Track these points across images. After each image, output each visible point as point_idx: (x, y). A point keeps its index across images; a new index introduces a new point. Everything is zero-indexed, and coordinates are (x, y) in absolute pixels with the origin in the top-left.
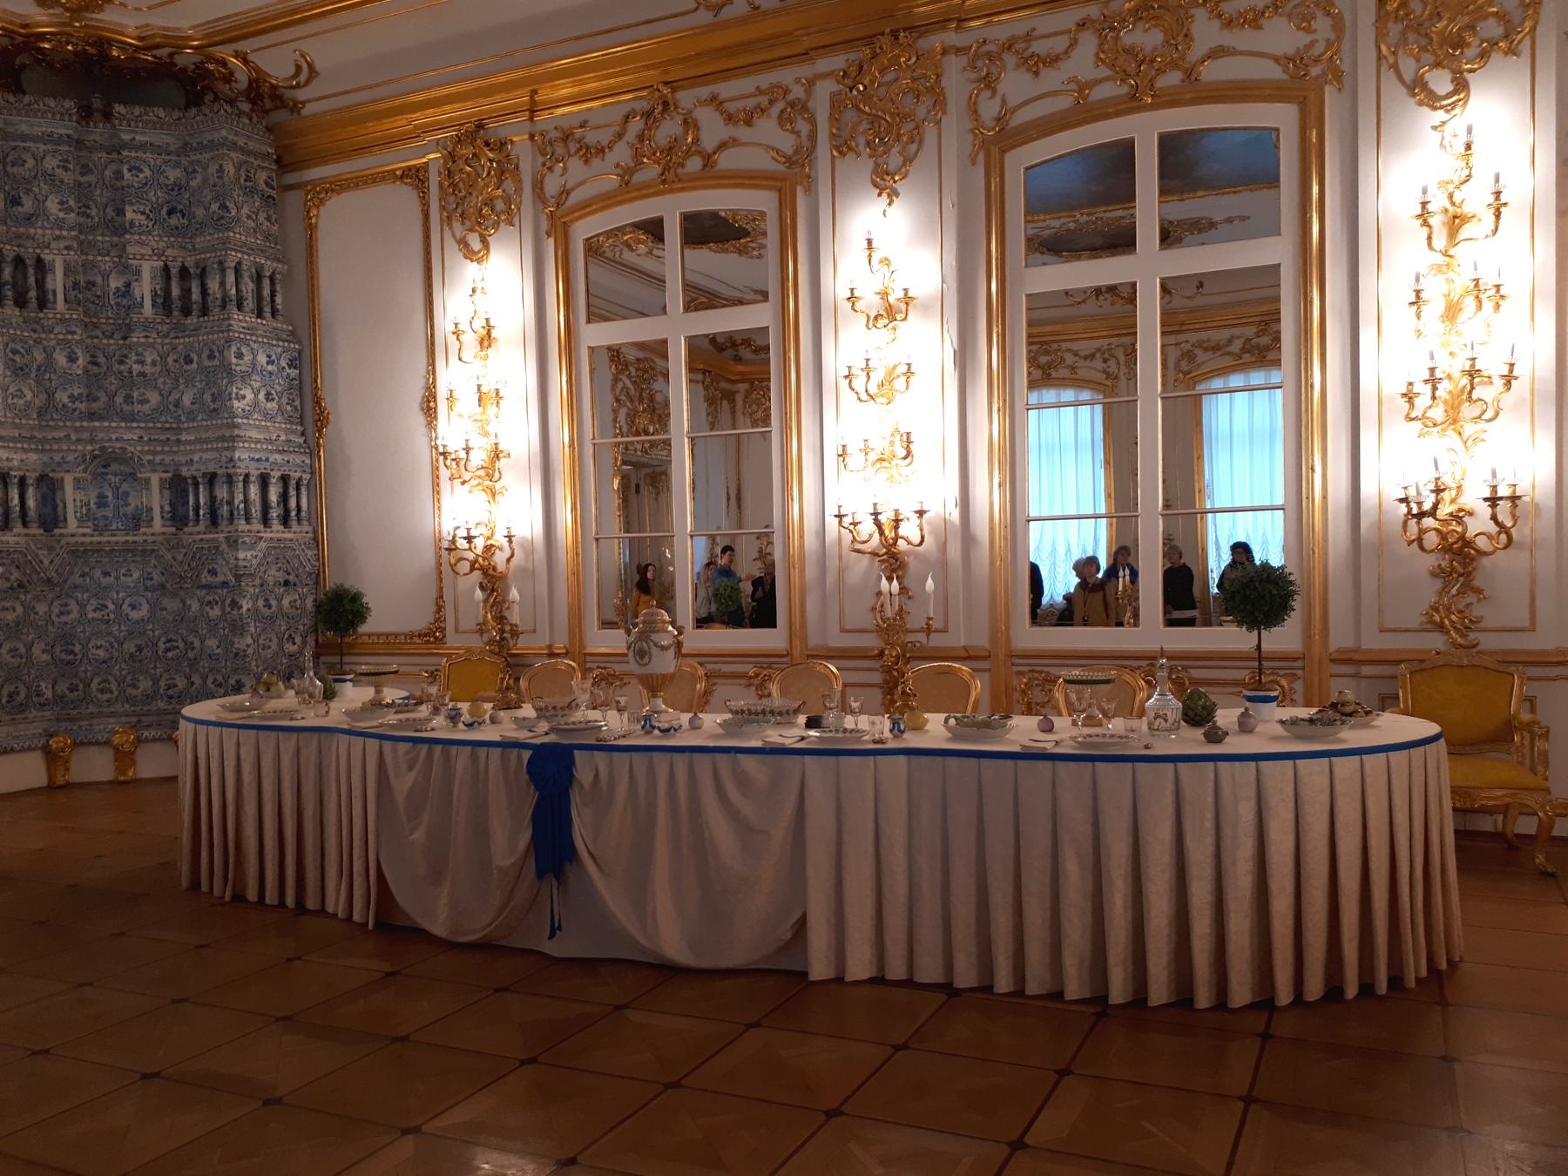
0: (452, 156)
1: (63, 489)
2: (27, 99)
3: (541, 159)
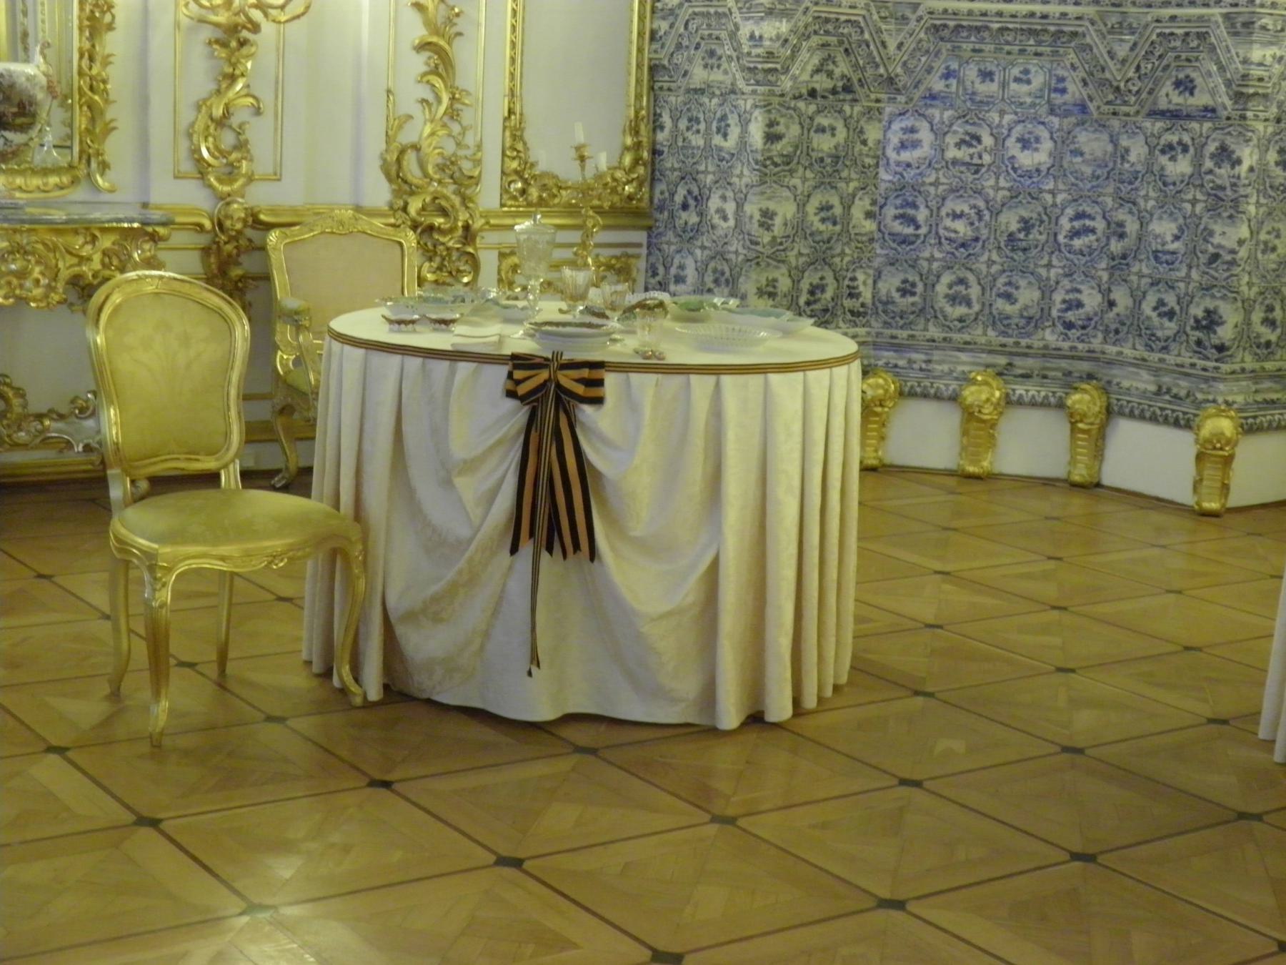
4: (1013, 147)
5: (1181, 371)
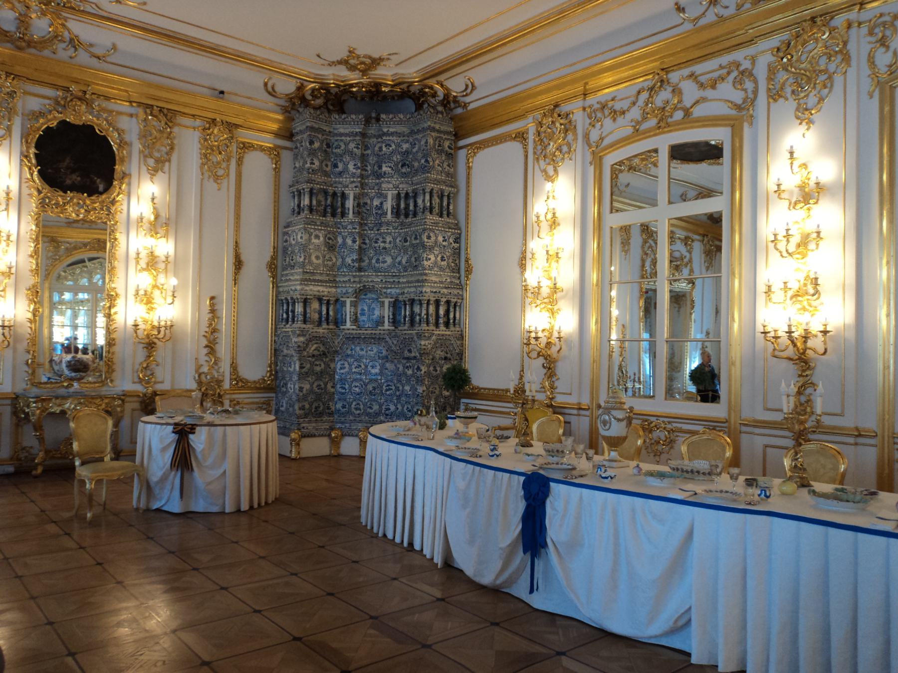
0: (541, 124)
3: (588, 121)
4: (369, 368)
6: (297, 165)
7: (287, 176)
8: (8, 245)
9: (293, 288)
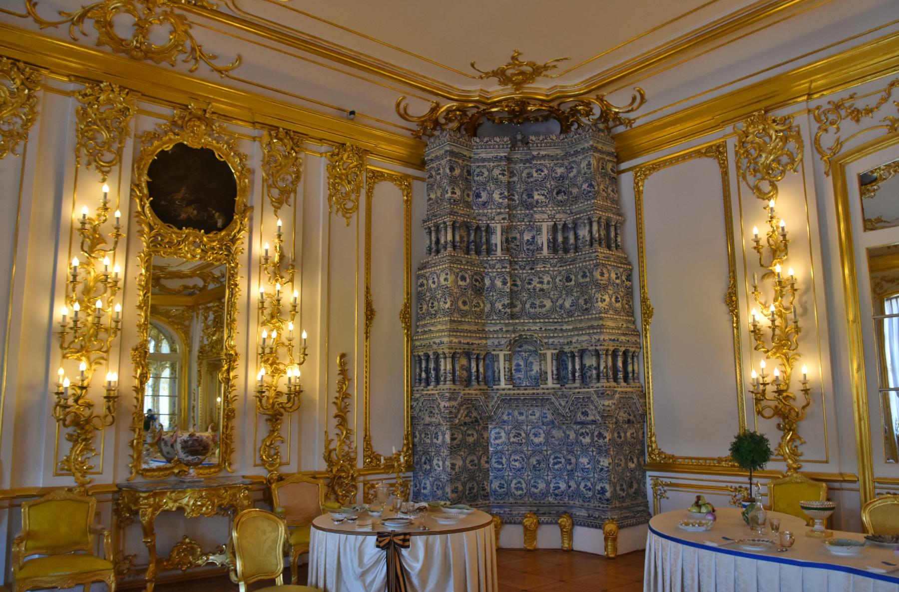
1: (498, 361)
2: (485, 140)
4: (532, 437)
5: (595, 509)
6: (433, 196)
7: (421, 208)
8: (114, 294)
9: (437, 341)
